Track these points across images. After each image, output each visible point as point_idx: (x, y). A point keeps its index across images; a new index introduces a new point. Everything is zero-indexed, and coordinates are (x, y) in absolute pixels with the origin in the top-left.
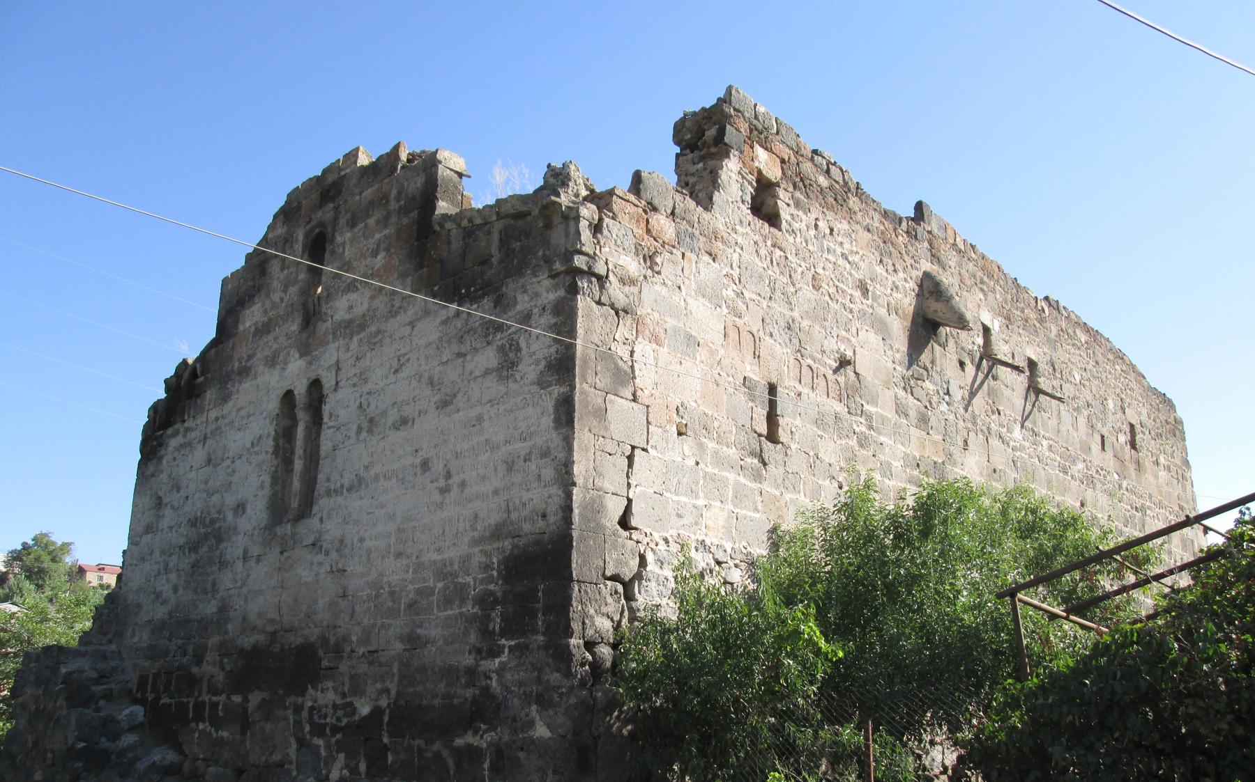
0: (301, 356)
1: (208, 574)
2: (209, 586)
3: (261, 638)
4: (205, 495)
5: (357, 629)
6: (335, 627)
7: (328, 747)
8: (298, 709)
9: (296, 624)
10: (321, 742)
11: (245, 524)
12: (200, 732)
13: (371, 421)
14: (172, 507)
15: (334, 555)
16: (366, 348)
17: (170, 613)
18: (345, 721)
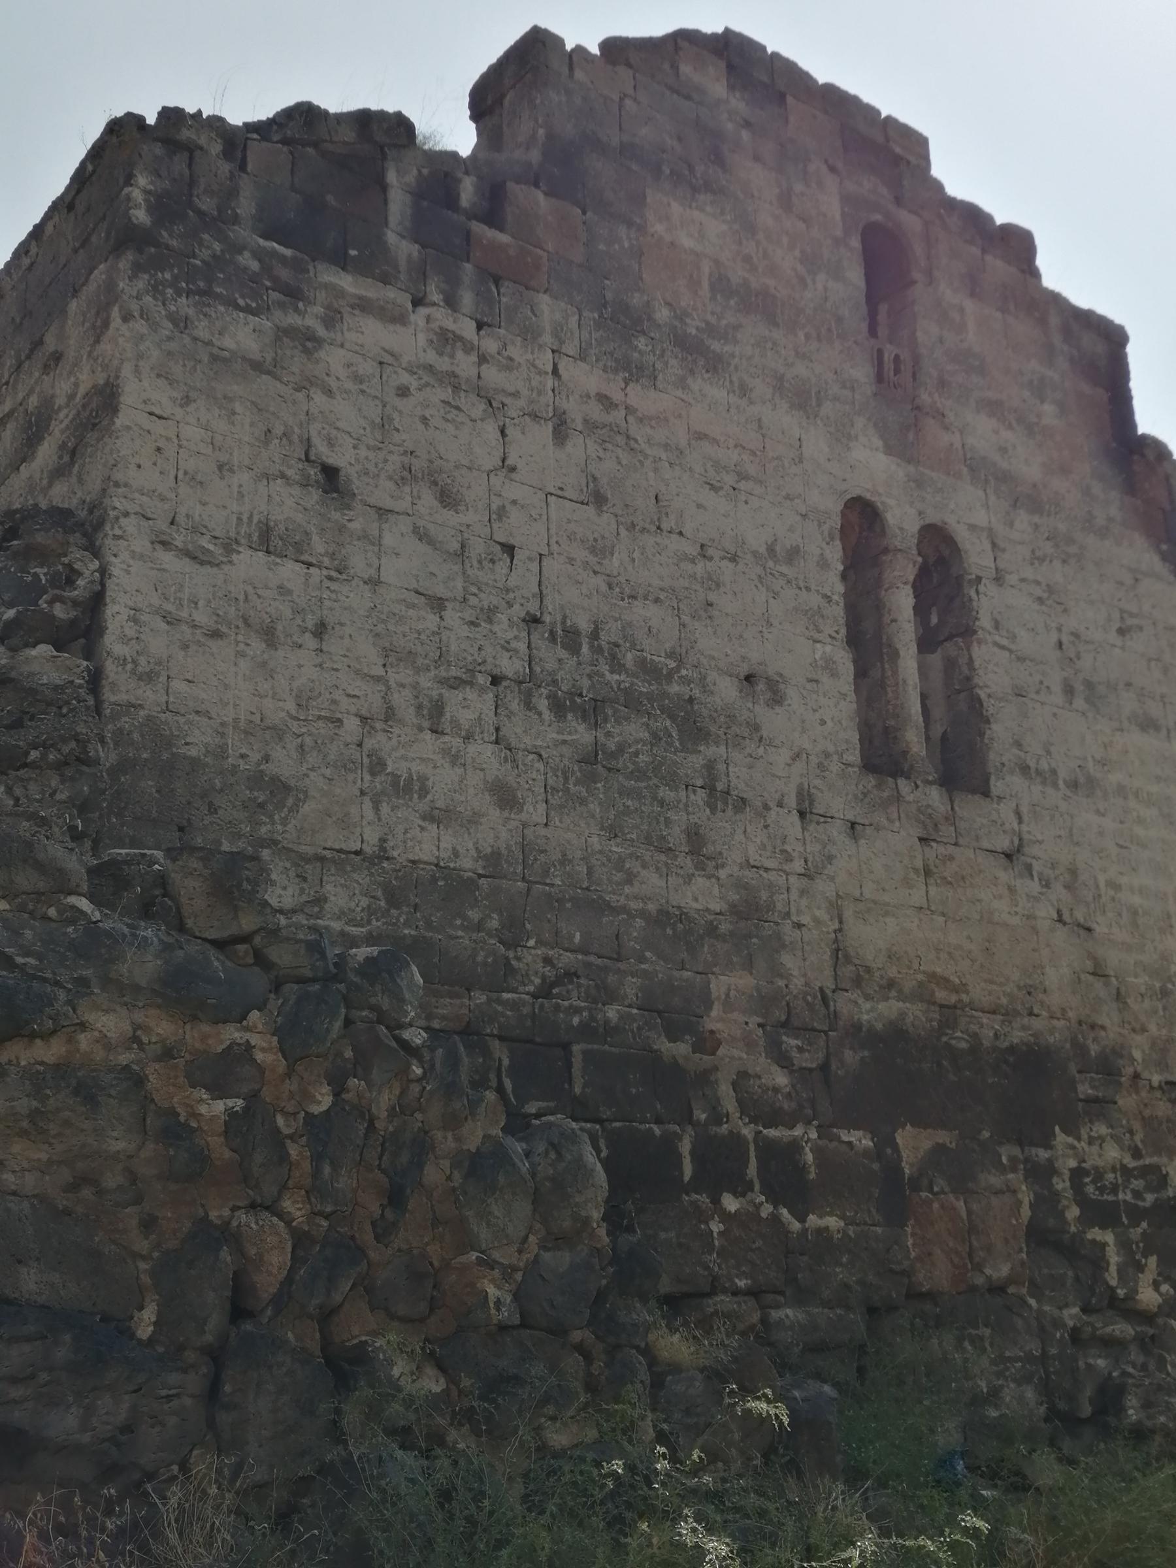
0: (889, 450)
1: (662, 803)
2: (676, 835)
3: (916, 1014)
4: (600, 582)
5: (1138, 1038)
6: (1093, 1027)
7: (1124, 1244)
8: (1041, 1174)
9: (1004, 1001)
10: (1109, 1237)
11: (773, 721)
12: (726, 1217)
13: (1089, 685)
14: (422, 535)
15: (1059, 892)
16: (1048, 548)
17: (493, 860)
18: (1150, 1198)
